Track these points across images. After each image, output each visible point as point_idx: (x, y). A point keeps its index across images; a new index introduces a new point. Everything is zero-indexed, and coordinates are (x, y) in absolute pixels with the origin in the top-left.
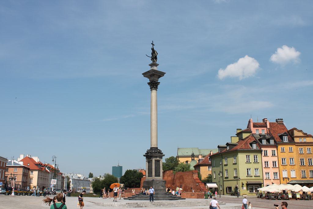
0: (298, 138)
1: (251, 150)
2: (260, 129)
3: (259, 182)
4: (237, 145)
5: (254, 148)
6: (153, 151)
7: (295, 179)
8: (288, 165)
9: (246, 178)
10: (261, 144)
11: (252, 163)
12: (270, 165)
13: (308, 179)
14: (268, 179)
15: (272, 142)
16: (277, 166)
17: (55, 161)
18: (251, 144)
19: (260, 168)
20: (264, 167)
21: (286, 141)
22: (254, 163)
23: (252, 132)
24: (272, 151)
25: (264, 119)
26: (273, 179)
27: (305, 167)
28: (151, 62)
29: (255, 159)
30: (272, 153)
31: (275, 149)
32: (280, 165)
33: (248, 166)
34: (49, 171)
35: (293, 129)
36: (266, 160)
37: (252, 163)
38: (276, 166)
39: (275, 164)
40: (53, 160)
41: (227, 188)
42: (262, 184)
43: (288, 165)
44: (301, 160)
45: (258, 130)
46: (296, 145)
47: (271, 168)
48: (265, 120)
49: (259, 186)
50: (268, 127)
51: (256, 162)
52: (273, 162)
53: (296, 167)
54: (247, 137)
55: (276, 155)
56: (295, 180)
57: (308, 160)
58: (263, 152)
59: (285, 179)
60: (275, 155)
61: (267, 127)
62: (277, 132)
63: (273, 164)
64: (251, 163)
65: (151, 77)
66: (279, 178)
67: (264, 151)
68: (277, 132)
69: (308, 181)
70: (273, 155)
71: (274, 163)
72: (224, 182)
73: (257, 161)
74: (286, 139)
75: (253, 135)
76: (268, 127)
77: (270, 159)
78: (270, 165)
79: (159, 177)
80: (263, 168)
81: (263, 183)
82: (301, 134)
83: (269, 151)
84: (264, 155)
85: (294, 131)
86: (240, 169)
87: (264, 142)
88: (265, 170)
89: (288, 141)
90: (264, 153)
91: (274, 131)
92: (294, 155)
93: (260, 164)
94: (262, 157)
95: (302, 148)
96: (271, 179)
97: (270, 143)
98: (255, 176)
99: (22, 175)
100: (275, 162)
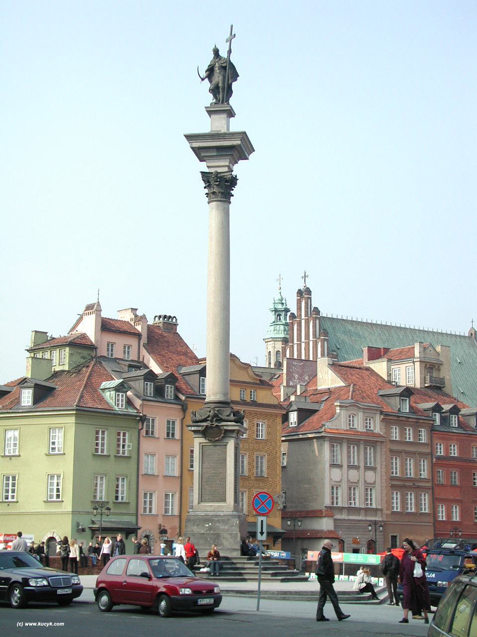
15: (169, 390)
22: (115, 456)
24: (168, 422)
28: (210, 99)
30: (168, 428)
37: (112, 457)
50: (144, 339)
55: (177, 436)
60: (173, 435)
64: (109, 456)
66: (176, 512)
70: (170, 435)
80: (140, 476)
84: (145, 435)
87: (150, 387)
94: (141, 438)
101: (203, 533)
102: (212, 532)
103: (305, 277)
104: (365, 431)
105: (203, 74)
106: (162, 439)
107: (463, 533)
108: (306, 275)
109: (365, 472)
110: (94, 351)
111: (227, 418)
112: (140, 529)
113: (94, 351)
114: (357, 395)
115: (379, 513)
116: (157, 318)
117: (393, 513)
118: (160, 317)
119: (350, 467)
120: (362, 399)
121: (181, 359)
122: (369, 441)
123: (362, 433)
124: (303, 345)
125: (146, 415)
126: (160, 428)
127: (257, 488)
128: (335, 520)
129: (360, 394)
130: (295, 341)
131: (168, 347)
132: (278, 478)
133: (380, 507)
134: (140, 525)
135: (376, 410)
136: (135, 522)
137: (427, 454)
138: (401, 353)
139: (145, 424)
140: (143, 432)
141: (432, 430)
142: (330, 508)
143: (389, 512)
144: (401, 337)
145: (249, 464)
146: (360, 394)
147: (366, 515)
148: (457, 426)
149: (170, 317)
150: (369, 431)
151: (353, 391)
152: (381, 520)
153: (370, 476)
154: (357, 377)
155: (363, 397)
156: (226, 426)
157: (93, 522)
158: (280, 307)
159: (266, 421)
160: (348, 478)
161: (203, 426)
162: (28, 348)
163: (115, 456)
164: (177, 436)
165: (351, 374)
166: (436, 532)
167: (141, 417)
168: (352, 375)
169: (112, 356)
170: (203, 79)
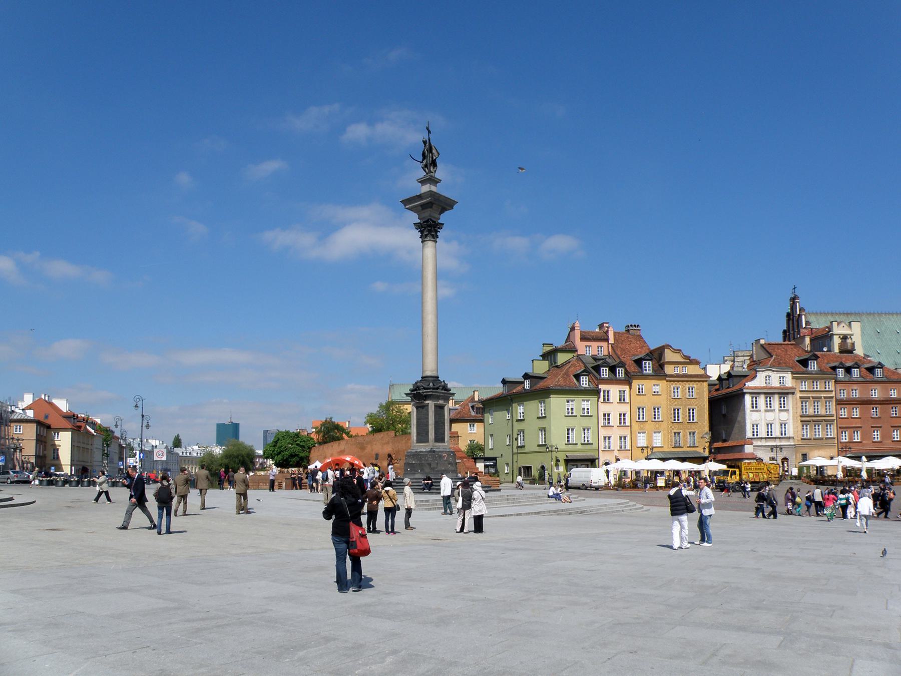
0: (672, 366)
1: (578, 390)
2: (595, 345)
3: (591, 455)
4: (545, 378)
5: (583, 384)
6: (431, 384)
7: (660, 450)
9: (565, 447)
10: (598, 377)
11: (579, 416)
12: (615, 420)
13: (685, 449)
14: (609, 449)
15: (621, 373)
16: (628, 423)
17: (140, 409)
18: (577, 377)
19: (593, 428)
21: (647, 372)
22: (581, 416)
23: (577, 351)
24: (620, 391)
25: (603, 323)
27: (681, 426)
30: (620, 396)
31: (626, 388)
33: (571, 422)
34: (93, 431)
35: (664, 346)
36: (607, 411)
37: (579, 416)
38: (625, 423)
39: (624, 419)
40: (136, 406)
41: (520, 469)
42: (597, 461)
44: (674, 410)
46: (667, 381)
48: (605, 325)
49: (589, 463)
50: (611, 341)
52: (620, 415)
53: (664, 425)
54: (568, 362)
55: (627, 400)
56: (661, 452)
57: (688, 412)
58: (602, 394)
59: (645, 449)
60: (624, 400)
61: (608, 342)
62: (630, 352)
63: (620, 419)
64: (576, 416)
66: (628, 447)
67: (604, 391)
68: (630, 352)
69: (684, 452)
70: (622, 400)
71: (622, 416)
72: (514, 455)
74: (648, 367)
75: (579, 358)
76: (611, 341)
77: (614, 409)
78: (615, 420)
79: (443, 444)
81: (598, 459)
82: (678, 358)
83: (614, 391)
84: (602, 401)
85: (666, 350)
86: (552, 428)
87: (605, 373)
88: (603, 430)
90: (604, 396)
91: (622, 350)
92: (662, 401)
93: (594, 419)
94: (599, 403)
95: (678, 386)
96: (614, 450)
97: (615, 375)
98: (582, 444)
99: (35, 441)
100: (624, 415)
101: (414, 463)
115: (791, 440)
117: (802, 439)
119: (766, 411)
120: (779, 365)
121: (637, 351)
122: (784, 393)
123: (775, 388)
128: (754, 446)
129: (778, 362)
132: (706, 422)
137: (832, 397)
140: (601, 399)
141: (835, 382)
142: (751, 438)
143: (800, 439)
144: (870, 319)
145: (683, 414)
146: (778, 362)
147: (781, 442)
148: (858, 376)
149: (635, 326)
151: (774, 360)
152: (793, 444)
153: (784, 416)
154: (782, 351)
157: (567, 456)
159: (695, 386)
162: (541, 354)
168: (778, 349)
169: (589, 354)
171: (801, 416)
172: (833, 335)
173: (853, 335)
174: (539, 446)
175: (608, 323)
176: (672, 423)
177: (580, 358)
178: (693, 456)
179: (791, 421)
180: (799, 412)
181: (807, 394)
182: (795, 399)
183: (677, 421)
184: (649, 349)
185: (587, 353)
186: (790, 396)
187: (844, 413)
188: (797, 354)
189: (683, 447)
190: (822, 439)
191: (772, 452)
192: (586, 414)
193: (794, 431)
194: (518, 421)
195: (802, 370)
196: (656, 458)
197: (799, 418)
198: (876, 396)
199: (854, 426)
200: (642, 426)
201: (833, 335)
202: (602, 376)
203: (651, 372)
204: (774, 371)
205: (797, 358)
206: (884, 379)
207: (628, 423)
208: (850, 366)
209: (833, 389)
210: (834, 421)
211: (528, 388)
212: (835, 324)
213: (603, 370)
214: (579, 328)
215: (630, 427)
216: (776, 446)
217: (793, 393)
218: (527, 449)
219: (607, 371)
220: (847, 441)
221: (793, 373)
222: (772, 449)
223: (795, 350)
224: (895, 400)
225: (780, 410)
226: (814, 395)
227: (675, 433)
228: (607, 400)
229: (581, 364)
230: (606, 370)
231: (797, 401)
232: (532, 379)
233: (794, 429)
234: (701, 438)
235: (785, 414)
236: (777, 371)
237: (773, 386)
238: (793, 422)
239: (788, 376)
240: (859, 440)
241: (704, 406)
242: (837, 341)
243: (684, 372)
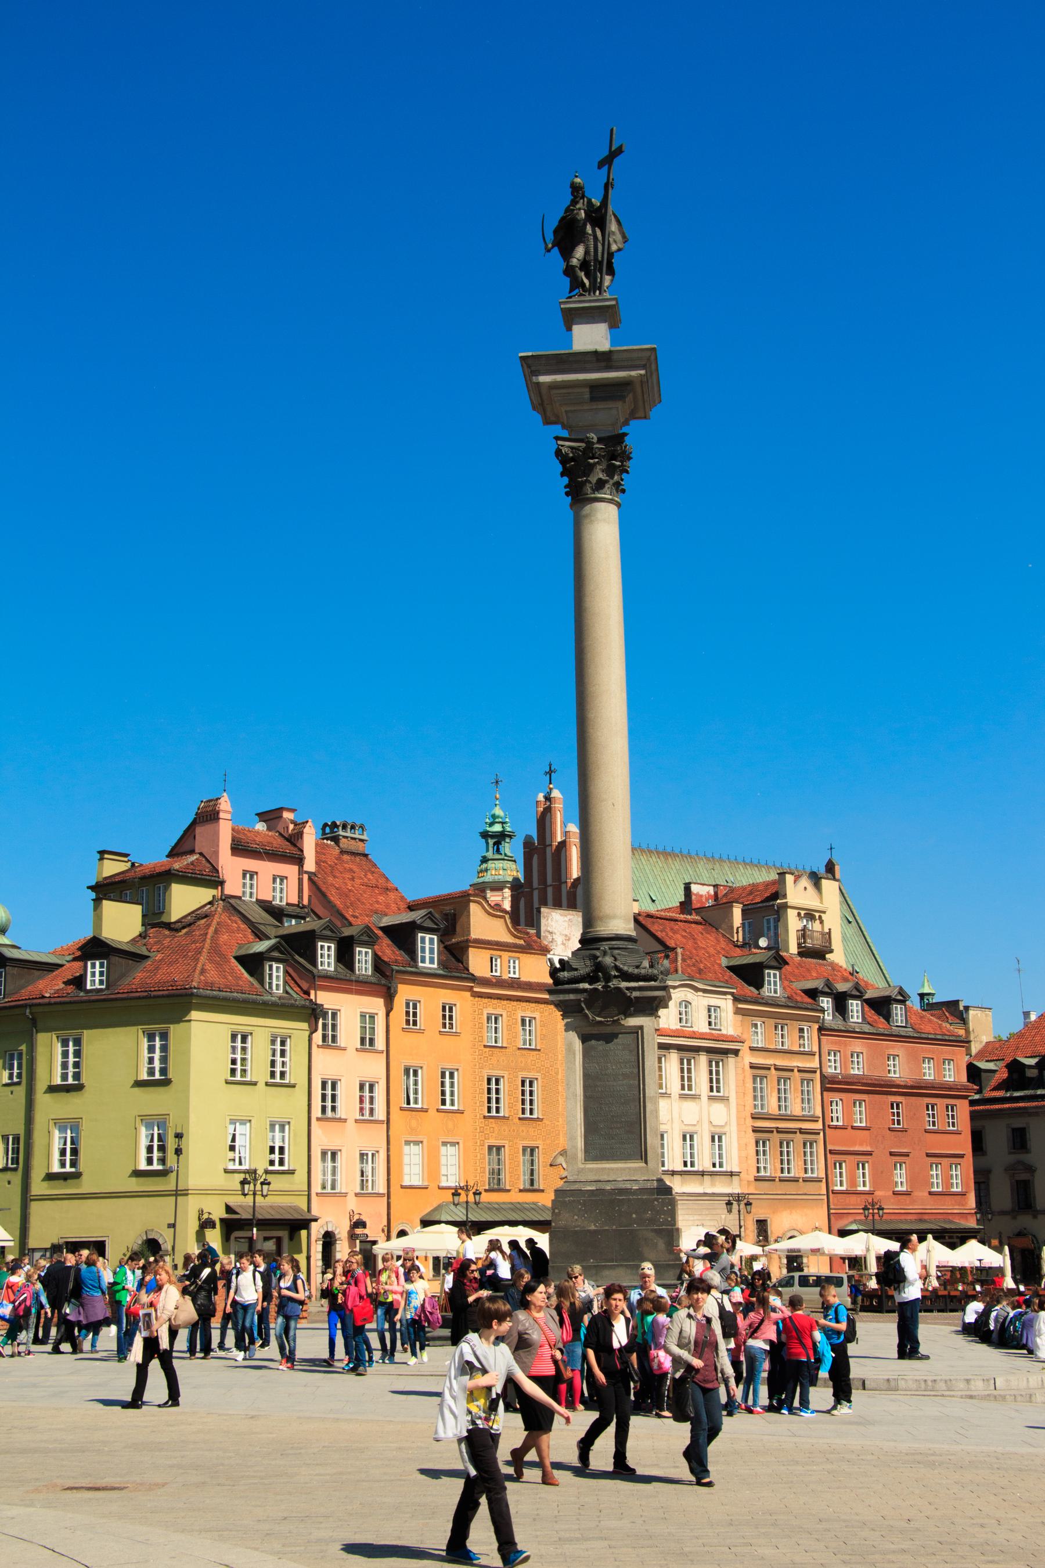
0: (486, 954)
2: (267, 869)
8: (432, 1112)
11: (261, 1085)
12: (347, 1103)
13: (515, 1197)
14: (331, 1191)
15: (364, 960)
18: (253, 964)
20: (320, 1115)
23: (222, 883)
24: (363, 1016)
25: (281, 809)
26: (356, 1195)
29: (273, 1063)
32: (394, 1109)
36: (330, 1074)
37: (261, 1085)
43: (432, 1112)
45: (253, 874)
47: (351, 1123)
49: (284, 1234)
51: (278, 1080)
52: (362, 1087)
55: (380, 1044)
60: (372, 1041)
64: (255, 1084)
65: (593, 399)
66: (382, 1188)
68: (363, 903)
70: (367, 1042)
71: (366, 1087)
73: (283, 1074)
74: (428, 945)
75: (231, 904)
76: (310, 865)
84: (321, 1043)
85: (473, 907)
87: (326, 956)
89: (438, 964)
90: (325, 1026)
93: (300, 1095)
100: (371, 1087)
101: (595, 1231)
102: (614, 1227)
103: (550, 772)
104: (708, 1031)
105: (550, 237)
106: (351, 1051)
107: (885, 1211)
108: (552, 769)
109: (709, 1106)
110: (220, 888)
111: (636, 971)
112: (316, 1220)
113: (220, 888)
114: (689, 966)
116: (328, 830)
118: (334, 825)
119: (682, 1097)
120: (700, 974)
121: (378, 902)
124: (550, 890)
125: (322, 1005)
126: (349, 1031)
127: (524, 1139)
129: (694, 965)
130: (535, 884)
131: (353, 879)
132: (560, 1119)
133: (736, 1169)
134: (315, 1212)
135: (725, 993)
136: (305, 1208)
138: (751, 893)
139: (321, 1021)
140: (318, 1037)
141: (820, 1029)
147: (713, 1185)
148: (860, 1020)
150: (713, 1032)
151: (684, 960)
153: (720, 1115)
154: (683, 936)
155: (700, 971)
156: (634, 989)
158: (497, 828)
160: (680, 1117)
161: (585, 990)
162: (93, 883)
163: (267, 1084)
164: (380, 1044)
165: (672, 929)
166: (832, 1211)
167: (314, 1010)
168: (675, 932)
170: (549, 251)
171: (754, 1117)
172: (785, 906)
173: (824, 912)
174: (138, 1174)
175: (293, 810)
176: (485, 1117)
177: (232, 906)
178: (542, 1219)
179: (734, 1128)
180: (749, 1109)
181: (765, 1058)
182: (740, 1071)
183: (494, 1113)
184: (402, 898)
185: (244, 893)
186: (731, 1060)
187: (838, 1113)
188: (719, 949)
189: (509, 1191)
190: (795, 1180)
191: (730, 1211)
192: (278, 1080)
193: (740, 1157)
194: (52, 1089)
195: (750, 994)
196: (448, 1223)
197: (750, 1122)
198: (897, 1075)
199: (857, 1148)
200: (414, 1123)
201: (785, 906)
202: (320, 968)
203: (435, 966)
204: (696, 989)
205: (724, 962)
206: (909, 1031)
207: (380, 1114)
208: (845, 992)
209: (816, 1049)
210: (819, 1134)
211: (98, 986)
212: (789, 879)
213: (322, 947)
214: (229, 816)
215: (385, 1125)
216: (739, 1198)
217: (736, 1052)
218: (86, 1185)
219: (333, 953)
220: (844, 1188)
221: (736, 999)
222: (729, 1204)
223: (708, 936)
224: (950, 1089)
225: (710, 1098)
226: (781, 1062)
227: (490, 1148)
228: (330, 1041)
229: (243, 926)
230: (329, 948)
231: (744, 1077)
232: (115, 959)
233: (739, 1150)
234: (551, 1165)
235: (718, 1107)
236: (705, 991)
237: (695, 1029)
238: (739, 1131)
239: (726, 1004)
240: (867, 1188)
241: (557, 1073)
242: (794, 923)
243: (512, 975)
